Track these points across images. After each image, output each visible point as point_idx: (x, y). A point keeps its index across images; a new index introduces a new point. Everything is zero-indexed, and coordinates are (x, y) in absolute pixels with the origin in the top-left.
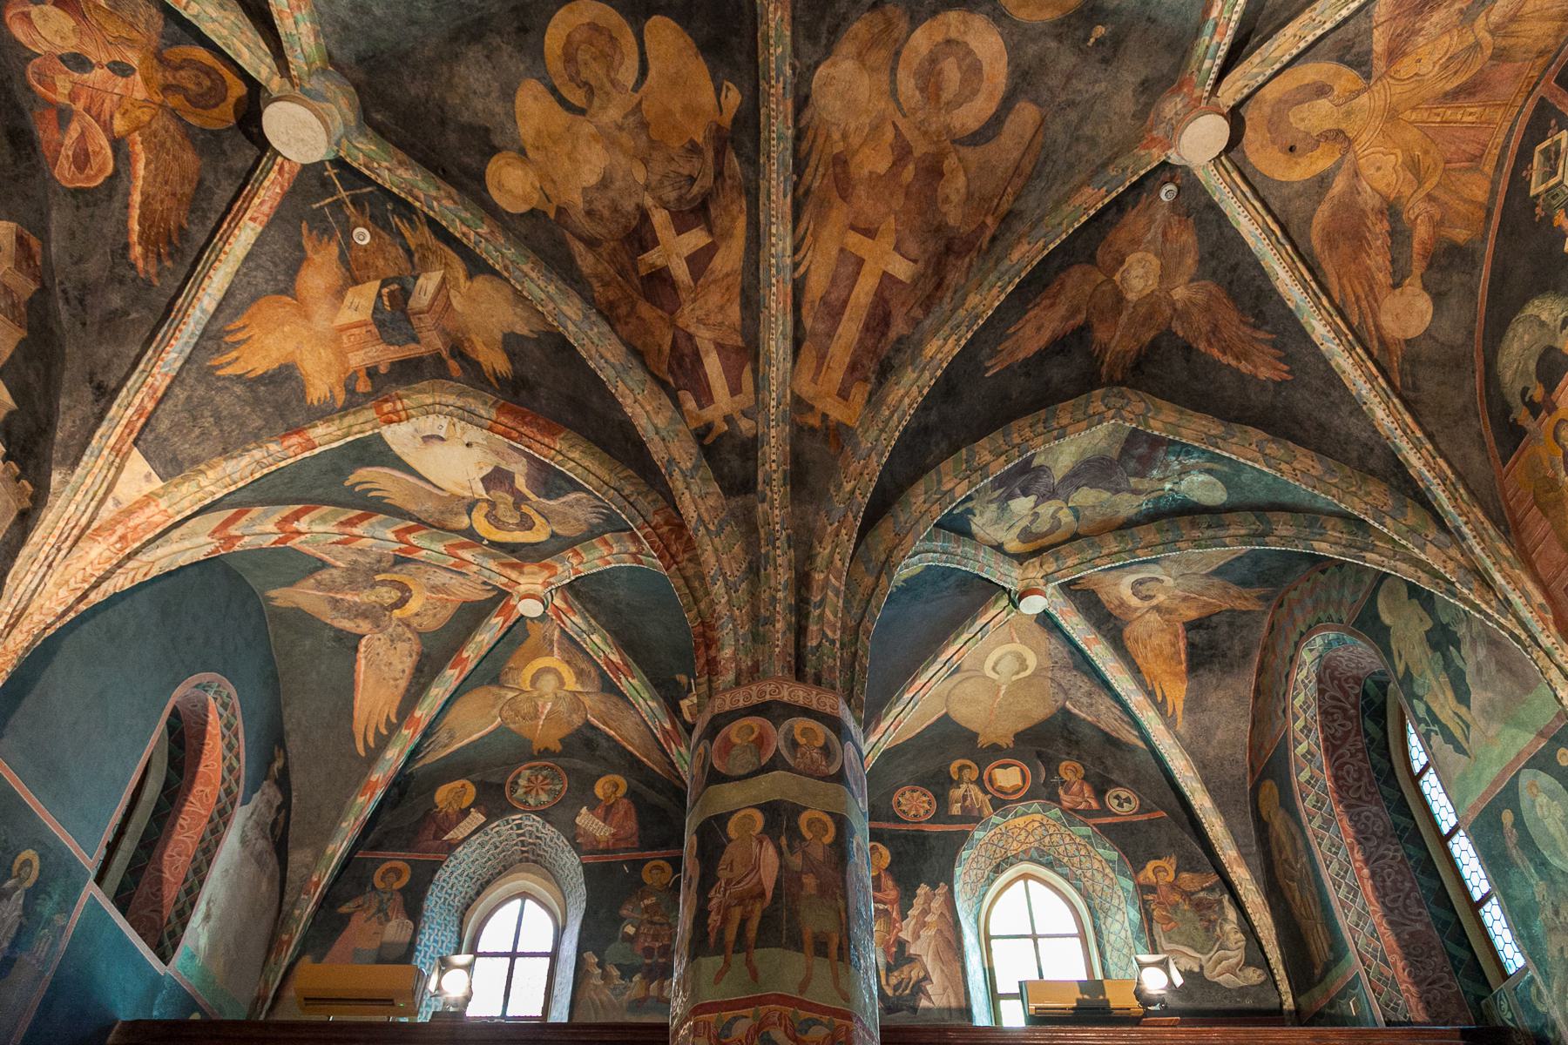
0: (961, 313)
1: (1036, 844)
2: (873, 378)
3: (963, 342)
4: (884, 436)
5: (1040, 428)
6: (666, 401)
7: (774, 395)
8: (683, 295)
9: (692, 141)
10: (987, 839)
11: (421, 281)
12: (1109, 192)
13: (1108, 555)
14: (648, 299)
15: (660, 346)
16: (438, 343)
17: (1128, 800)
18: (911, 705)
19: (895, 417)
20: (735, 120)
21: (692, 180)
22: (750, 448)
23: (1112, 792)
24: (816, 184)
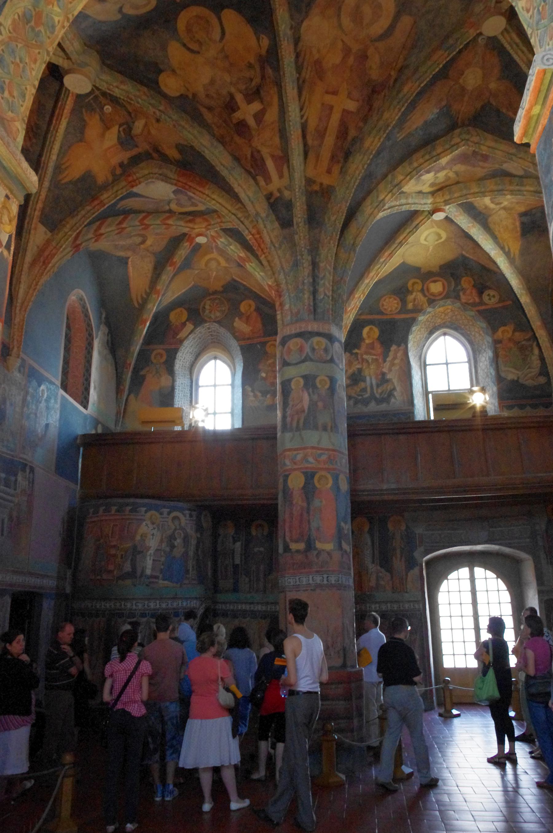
0: (381, 123)
1: (449, 320)
2: (342, 160)
3: (382, 140)
4: (348, 192)
5: (427, 157)
6: (252, 182)
7: (297, 186)
8: (253, 133)
9: (249, 62)
10: (425, 320)
11: (136, 124)
12: (449, 55)
13: (474, 193)
14: (239, 135)
15: (246, 155)
16: (147, 147)
17: (494, 296)
18: (383, 265)
19: (353, 181)
20: (267, 51)
21: (251, 80)
22: (289, 205)
23: (486, 292)
24: (307, 77)
